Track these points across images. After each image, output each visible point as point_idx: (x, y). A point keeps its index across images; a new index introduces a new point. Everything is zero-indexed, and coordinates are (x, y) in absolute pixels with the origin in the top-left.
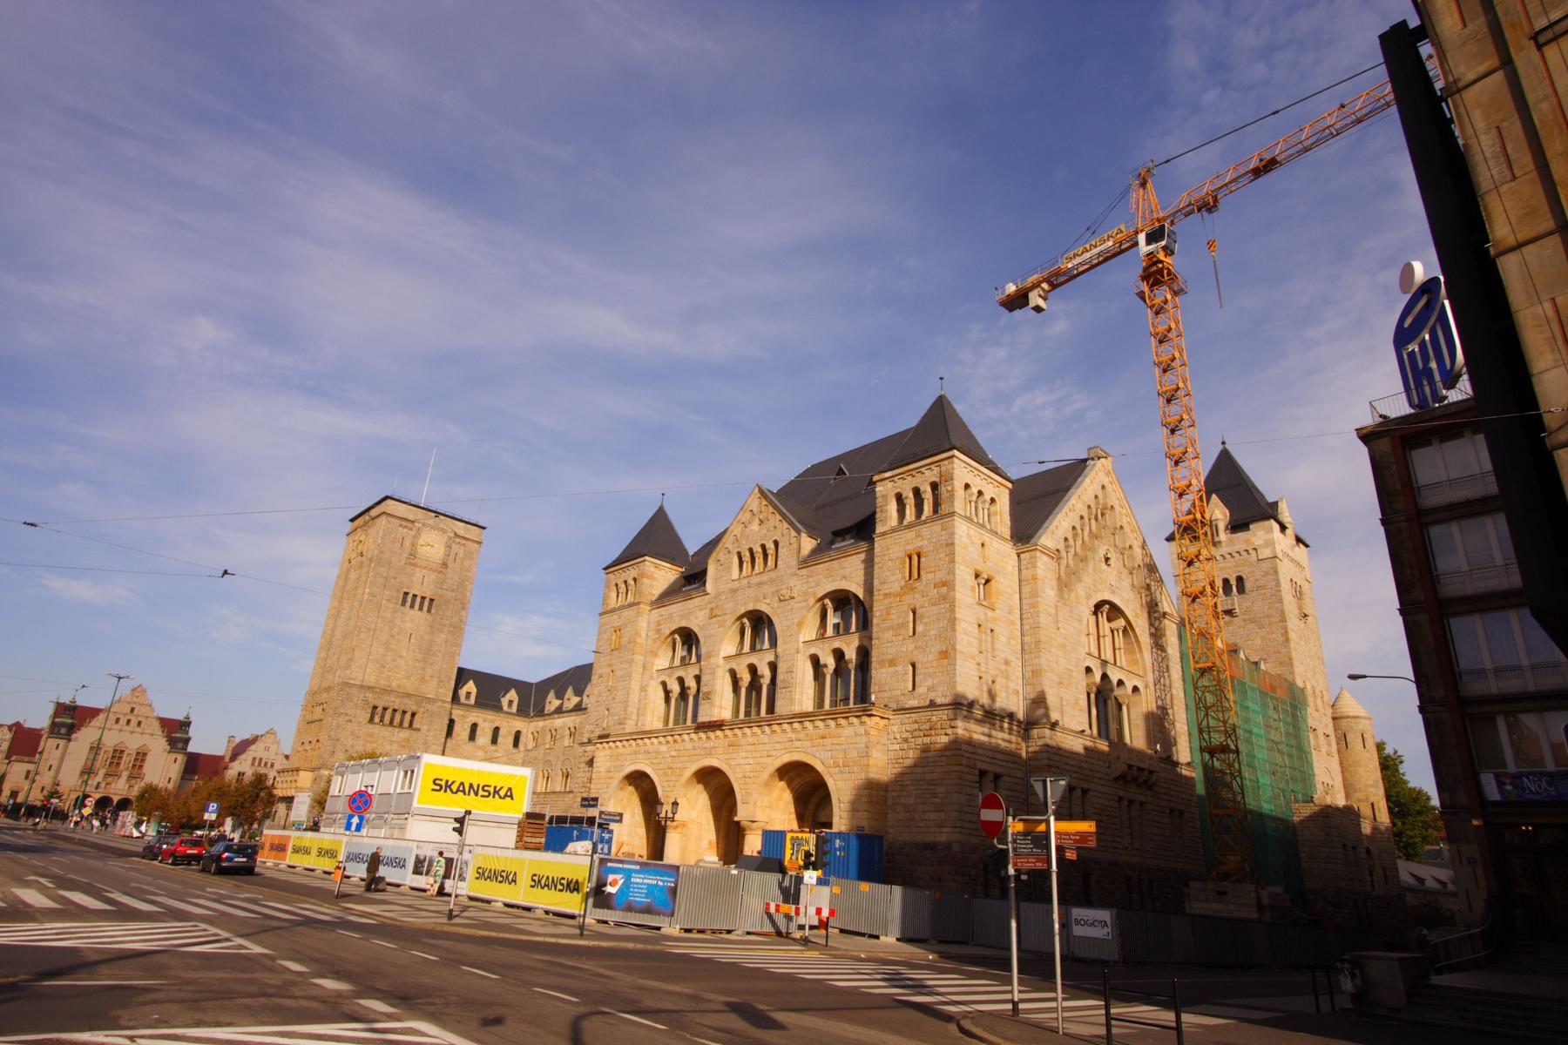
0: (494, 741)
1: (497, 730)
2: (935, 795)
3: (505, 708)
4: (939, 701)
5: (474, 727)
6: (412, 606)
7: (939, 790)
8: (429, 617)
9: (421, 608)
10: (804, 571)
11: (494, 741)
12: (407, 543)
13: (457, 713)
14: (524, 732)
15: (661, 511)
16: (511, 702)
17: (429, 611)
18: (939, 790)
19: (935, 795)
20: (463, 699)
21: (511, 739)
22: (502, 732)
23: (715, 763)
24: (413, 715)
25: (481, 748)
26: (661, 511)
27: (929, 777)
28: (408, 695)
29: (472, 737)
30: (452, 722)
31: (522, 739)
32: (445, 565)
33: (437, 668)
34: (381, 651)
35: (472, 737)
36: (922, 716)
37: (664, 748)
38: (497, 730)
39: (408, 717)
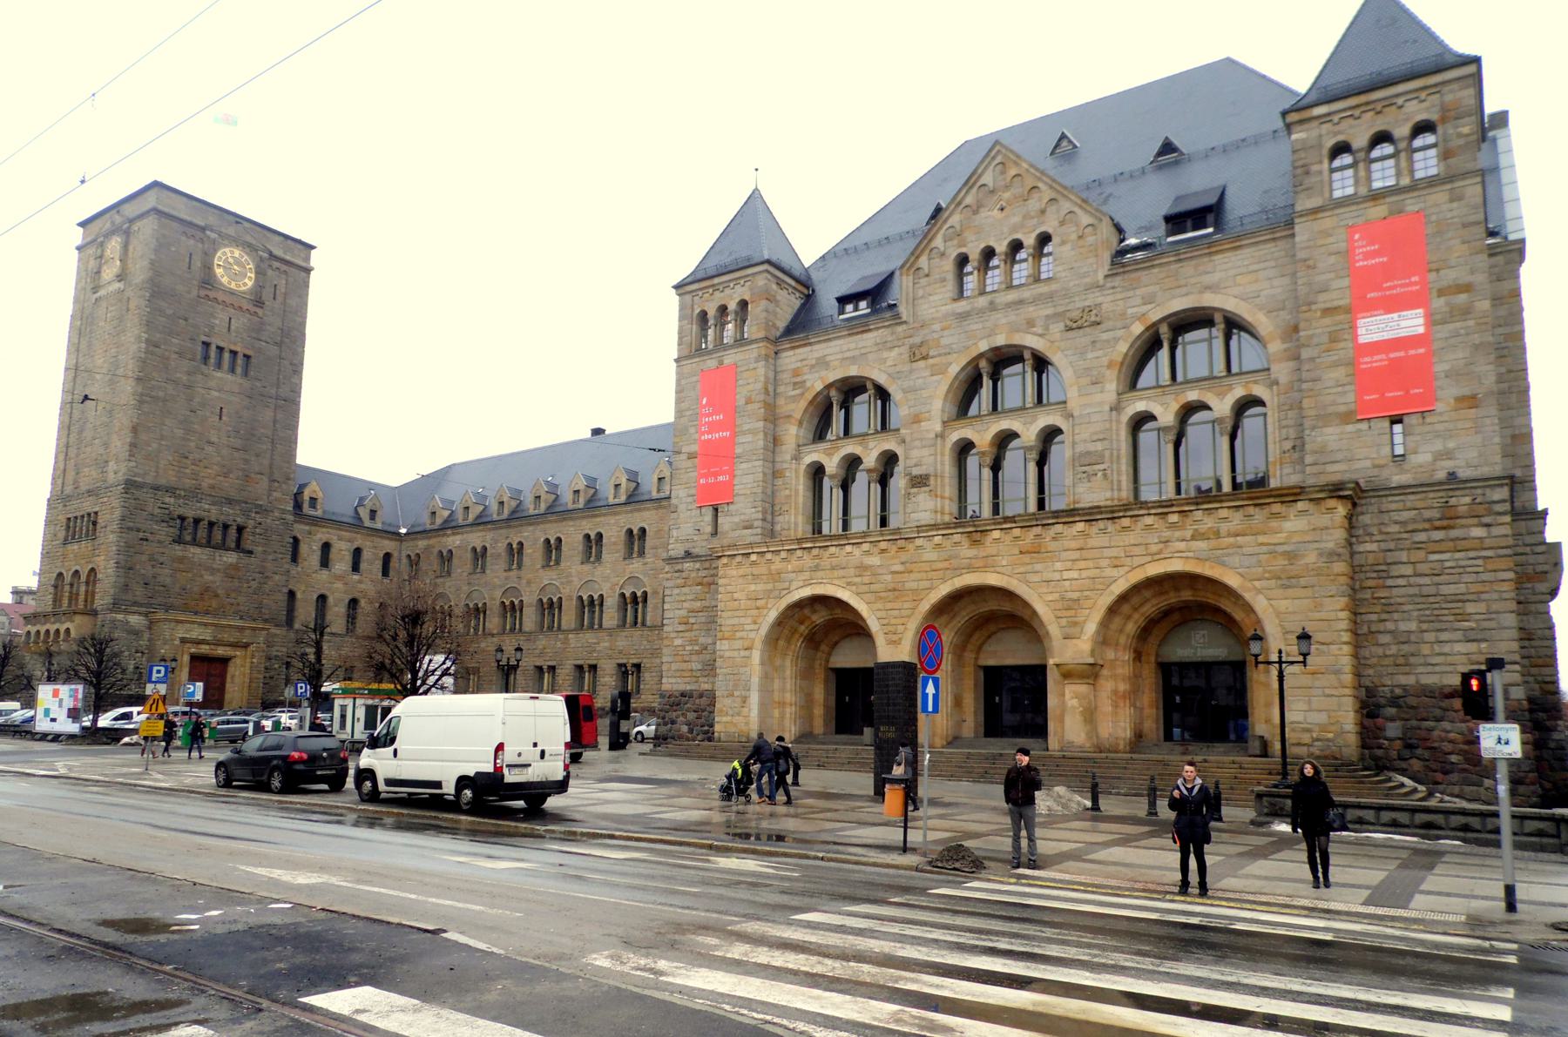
0: (356, 567)
1: (357, 553)
2: (1464, 617)
3: (367, 523)
4: (1463, 473)
5: (326, 547)
6: (219, 365)
7: (1470, 608)
8: (246, 384)
9: (232, 370)
10: (1117, 281)
11: (356, 567)
12: (197, 264)
13: (300, 529)
14: (395, 554)
15: (755, 199)
16: (373, 513)
17: (246, 374)
18: (1470, 608)
19: (1464, 617)
20: (306, 509)
21: (379, 564)
22: (366, 555)
23: (992, 580)
24: (240, 529)
25: (339, 578)
26: (755, 199)
27: (1451, 589)
28: (230, 501)
29: (325, 562)
30: (296, 541)
31: (394, 564)
32: (259, 303)
33: (266, 462)
34: (179, 432)
35: (325, 562)
36: (1435, 499)
37: (875, 560)
38: (357, 553)
39: (233, 532)
